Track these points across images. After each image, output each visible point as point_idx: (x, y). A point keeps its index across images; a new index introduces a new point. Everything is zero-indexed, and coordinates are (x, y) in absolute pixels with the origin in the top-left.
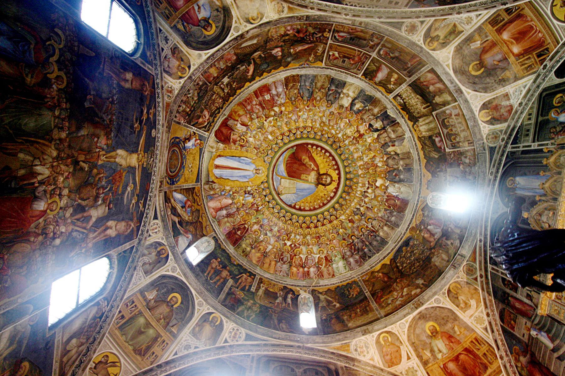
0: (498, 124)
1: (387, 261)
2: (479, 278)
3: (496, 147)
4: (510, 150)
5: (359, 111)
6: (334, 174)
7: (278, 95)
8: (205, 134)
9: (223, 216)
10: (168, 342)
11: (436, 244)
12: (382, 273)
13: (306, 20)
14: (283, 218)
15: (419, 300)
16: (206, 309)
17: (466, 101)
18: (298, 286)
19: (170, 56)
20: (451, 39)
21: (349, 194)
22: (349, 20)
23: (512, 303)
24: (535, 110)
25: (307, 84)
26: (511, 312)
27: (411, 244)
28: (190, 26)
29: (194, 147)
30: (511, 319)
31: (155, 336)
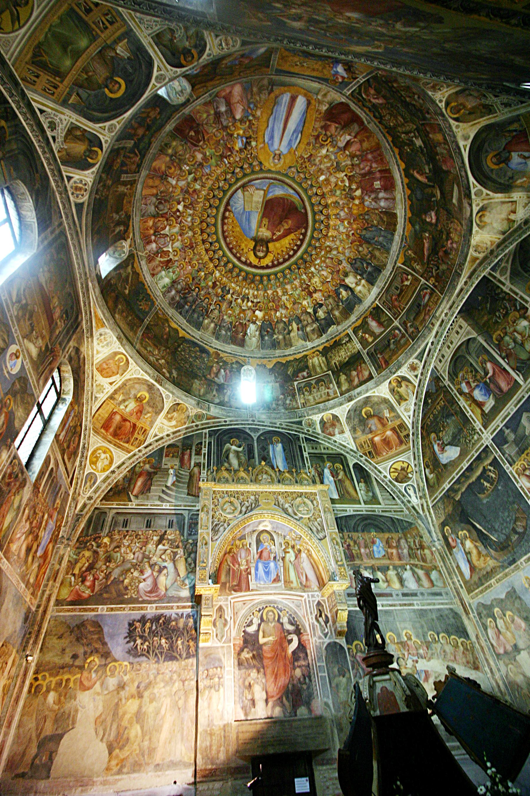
1: (182, 333)
5: (338, 294)
6: (267, 261)
7: (376, 199)
8: (348, 90)
9: (217, 108)
10: (56, 95)
11: (210, 380)
12: (169, 331)
13: (456, 271)
14: (212, 195)
16: (106, 138)
17: (341, 404)
18: (134, 234)
19: (483, 101)
21: (245, 279)
22: (440, 315)
24: (331, 452)
25: (381, 239)
27: (204, 355)
28: (509, 139)
29: (332, 72)
31: (62, 70)
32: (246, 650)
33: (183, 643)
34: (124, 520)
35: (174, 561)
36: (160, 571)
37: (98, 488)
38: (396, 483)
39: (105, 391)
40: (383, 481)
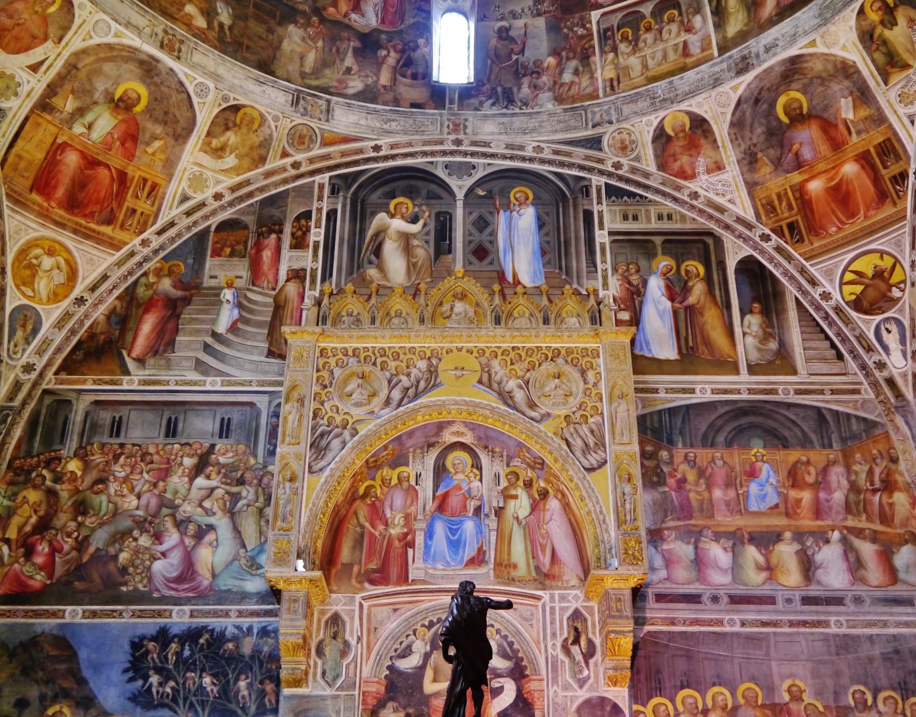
0: (655, 150)
2: (288, 161)
3: (601, 150)
4: (594, 183)
15: (182, 42)
17: (717, 82)
20: (877, 55)
23: (266, 242)
26: (246, 243)
30: (232, 246)
32: (390, 705)
33: (250, 686)
34: (112, 419)
35: (232, 514)
36: (200, 535)
37: (47, 342)
38: (854, 314)
39: (24, 90)
40: (818, 308)
